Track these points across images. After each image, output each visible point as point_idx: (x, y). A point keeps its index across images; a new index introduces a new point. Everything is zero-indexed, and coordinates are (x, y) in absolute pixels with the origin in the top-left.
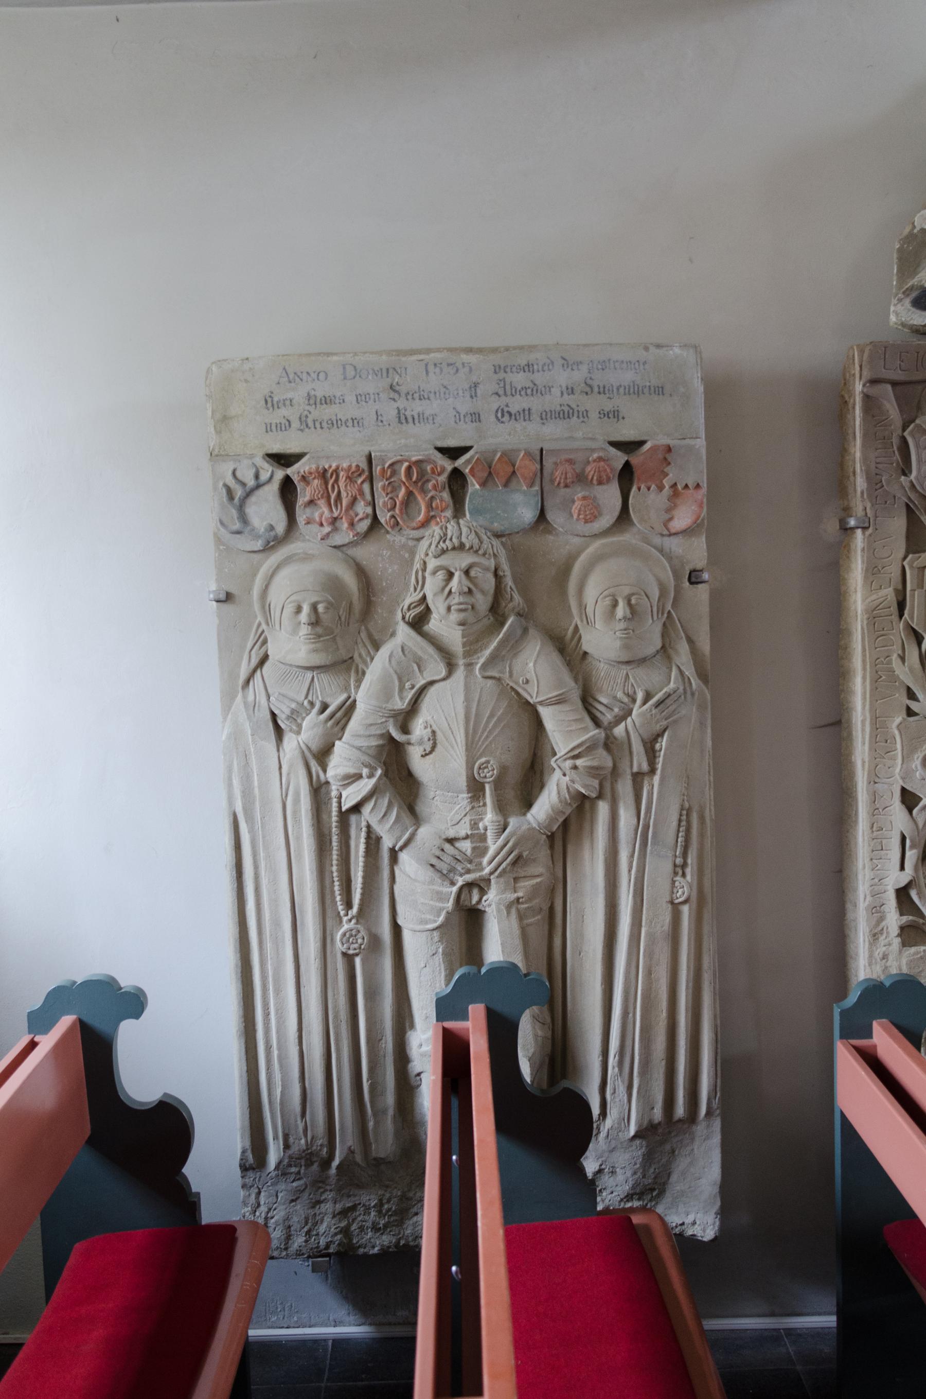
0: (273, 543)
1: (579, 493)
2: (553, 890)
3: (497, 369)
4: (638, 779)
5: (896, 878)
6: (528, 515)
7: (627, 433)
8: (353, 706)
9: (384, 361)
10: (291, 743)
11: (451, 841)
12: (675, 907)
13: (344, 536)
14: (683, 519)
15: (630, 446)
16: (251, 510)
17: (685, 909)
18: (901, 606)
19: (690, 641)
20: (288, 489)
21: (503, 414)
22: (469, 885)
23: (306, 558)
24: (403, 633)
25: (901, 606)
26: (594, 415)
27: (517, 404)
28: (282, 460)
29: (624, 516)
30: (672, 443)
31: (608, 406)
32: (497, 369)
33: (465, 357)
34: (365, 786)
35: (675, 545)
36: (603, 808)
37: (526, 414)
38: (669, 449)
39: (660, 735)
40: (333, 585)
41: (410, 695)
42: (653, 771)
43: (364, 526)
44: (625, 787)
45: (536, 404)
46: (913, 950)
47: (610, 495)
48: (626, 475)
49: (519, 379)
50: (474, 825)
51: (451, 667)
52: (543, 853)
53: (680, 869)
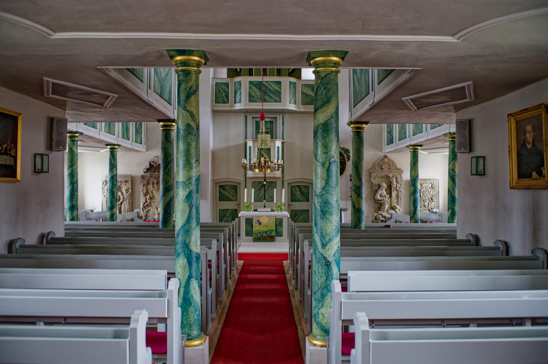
0: (105, 185)
4: (126, 200)
5: (142, 207)
6: (120, 184)
7: (126, 179)
10: (106, 197)
14: (129, 185)
15: (126, 180)
20: (106, 182)
25: (142, 190)
28: (106, 181)
29: (126, 185)
35: (129, 186)
36: (124, 202)
37: (120, 178)
44: (125, 200)
45: (120, 178)
47: (125, 183)
48: (126, 182)
53: (128, 206)
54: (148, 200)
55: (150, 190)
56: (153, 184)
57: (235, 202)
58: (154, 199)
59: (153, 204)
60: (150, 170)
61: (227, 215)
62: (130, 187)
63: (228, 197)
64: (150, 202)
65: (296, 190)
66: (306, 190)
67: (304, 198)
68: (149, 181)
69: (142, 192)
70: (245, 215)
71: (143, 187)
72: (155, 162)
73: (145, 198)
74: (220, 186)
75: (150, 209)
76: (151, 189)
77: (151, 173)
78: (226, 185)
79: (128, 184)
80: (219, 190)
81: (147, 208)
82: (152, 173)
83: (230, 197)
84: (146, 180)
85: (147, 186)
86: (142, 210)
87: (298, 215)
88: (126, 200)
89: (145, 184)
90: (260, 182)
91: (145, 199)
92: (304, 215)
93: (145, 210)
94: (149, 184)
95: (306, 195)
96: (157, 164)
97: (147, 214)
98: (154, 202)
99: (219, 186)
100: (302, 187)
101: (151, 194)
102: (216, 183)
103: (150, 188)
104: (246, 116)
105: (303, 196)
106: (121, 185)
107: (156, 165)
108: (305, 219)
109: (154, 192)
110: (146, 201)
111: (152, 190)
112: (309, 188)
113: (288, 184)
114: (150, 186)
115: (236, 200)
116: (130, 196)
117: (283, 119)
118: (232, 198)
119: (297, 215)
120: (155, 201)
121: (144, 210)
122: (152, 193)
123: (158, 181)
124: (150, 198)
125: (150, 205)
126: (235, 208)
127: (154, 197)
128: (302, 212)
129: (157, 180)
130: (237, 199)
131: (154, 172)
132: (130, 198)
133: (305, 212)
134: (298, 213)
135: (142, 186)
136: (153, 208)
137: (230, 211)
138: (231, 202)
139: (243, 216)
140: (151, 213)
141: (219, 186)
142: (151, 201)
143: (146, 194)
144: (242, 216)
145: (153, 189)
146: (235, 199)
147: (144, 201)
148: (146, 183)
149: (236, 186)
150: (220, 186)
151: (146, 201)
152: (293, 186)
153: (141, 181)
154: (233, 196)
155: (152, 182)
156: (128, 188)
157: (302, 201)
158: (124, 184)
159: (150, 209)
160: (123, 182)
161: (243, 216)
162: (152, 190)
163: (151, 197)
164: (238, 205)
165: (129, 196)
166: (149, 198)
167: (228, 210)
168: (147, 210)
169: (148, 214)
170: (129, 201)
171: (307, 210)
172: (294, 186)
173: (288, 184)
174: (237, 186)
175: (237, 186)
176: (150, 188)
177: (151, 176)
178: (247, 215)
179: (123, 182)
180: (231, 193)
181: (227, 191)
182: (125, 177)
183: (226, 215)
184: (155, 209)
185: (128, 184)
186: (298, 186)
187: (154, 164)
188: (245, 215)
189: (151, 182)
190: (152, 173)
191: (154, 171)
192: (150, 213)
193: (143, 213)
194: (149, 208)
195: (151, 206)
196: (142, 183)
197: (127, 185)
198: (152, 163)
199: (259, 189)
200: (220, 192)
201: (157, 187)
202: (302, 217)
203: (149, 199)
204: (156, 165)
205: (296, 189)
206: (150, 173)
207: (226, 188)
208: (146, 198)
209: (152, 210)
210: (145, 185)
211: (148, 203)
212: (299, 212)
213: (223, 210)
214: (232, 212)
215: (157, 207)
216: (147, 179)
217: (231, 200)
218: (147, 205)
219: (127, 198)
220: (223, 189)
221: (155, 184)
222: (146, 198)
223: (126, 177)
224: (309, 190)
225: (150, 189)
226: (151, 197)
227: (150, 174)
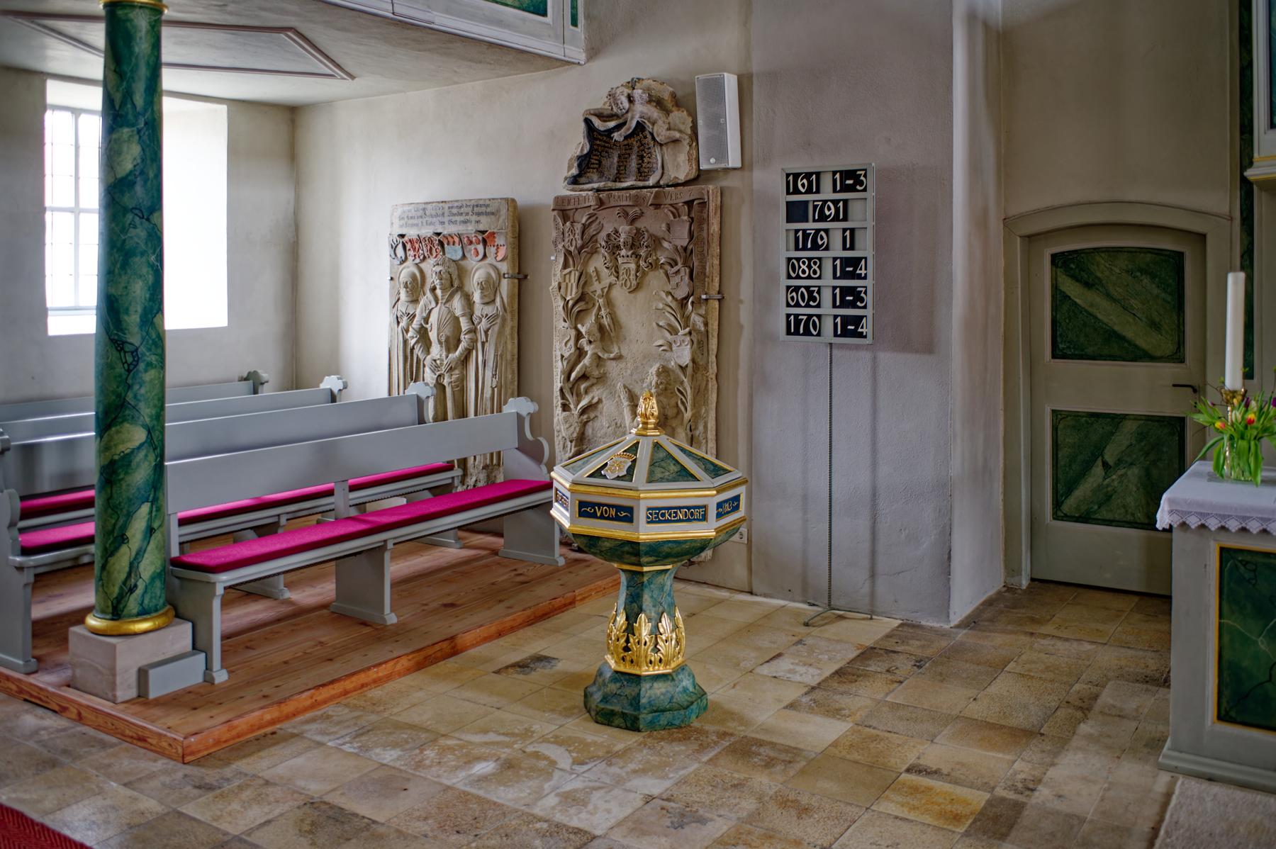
0: (403, 262)
1: (472, 247)
2: (462, 380)
3: (449, 208)
6: (460, 255)
7: (481, 228)
8: (415, 316)
9: (424, 206)
11: (435, 361)
12: (493, 389)
13: (417, 261)
16: (397, 251)
17: (496, 389)
18: (560, 288)
19: (502, 298)
21: (450, 222)
22: (440, 376)
23: (408, 267)
24: (429, 294)
25: (560, 288)
26: (473, 222)
27: (454, 219)
28: (402, 236)
29: (485, 256)
30: (495, 231)
31: (478, 219)
32: (449, 208)
33: (441, 204)
34: (415, 340)
35: (499, 265)
36: (474, 352)
38: (494, 233)
39: (489, 329)
40: (414, 277)
41: (427, 311)
42: (487, 341)
43: (422, 257)
45: (458, 218)
46: (565, 413)
47: (480, 248)
48: (485, 242)
49: (455, 211)
50: (441, 356)
51: (437, 303)
52: (460, 367)
53: (494, 375)
54: (587, 348)
55: (597, 287)
56: (614, 249)
57: (1167, 372)
58: (618, 337)
59: (613, 368)
60: (600, 162)
61: (1110, 455)
62: (504, 268)
63: (1112, 336)
64: (598, 360)
68: (592, 230)
69: (559, 298)
70: (1213, 524)
71: (565, 266)
72: (611, 117)
73: (573, 333)
74: (1059, 260)
75: (600, 401)
76: (605, 283)
77: (602, 184)
79: (493, 250)
80: (1055, 288)
81: (586, 392)
82: (610, 184)
83: (1129, 333)
84: (578, 227)
85: (586, 264)
86: (560, 402)
88: (483, 344)
89: (572, 249)
91: (572, 343)
93: (576, 407)
94: (594, 252)
96: (624, 124)
97: (585, 424)
98: (619, 358)
99: (1054, 257)
101: (603, 312)
102: (1030, 239)
103: (596, 270)
106: (464, 257)
107: (624, 132)
109: (619, 294)
110: (580, 353)
111: (611, 286)
114: (598, 263)
115: (1177, 357)
116: (504, 320)
118: (1144, 340)
120: (624, 353)
121: (572, 406)
122: (609, 303)
123: (638, 230)
124: (598, 335)
125: (596, 373)
126: (1168, 411)
127: (620, 327)
129: (633, 222)
130: (1180, 344)
131: (617, 179)
132: (501, 333)
135: (561, 260)
136: (613, 394)
137: (1130, 427)
138: (1139, 370)
139: (1193, 522)
140: (605, 424)
141: (1054, 257)
142: (600, 354)
143: (576, 309)
144: (1184, 525)
145: (613, 279)
146: (1168, 348)
147: (569, 351)
148: (580, 242)
149: (1177, 259)
150: (1059, 260)
151: (580, 353)
153: (554, 234)
154: (1154, 326)
155: (609, 235)
156: (493, 275)
158: (477, 254)
159: (600, 401)
160: (471, 243)
161: (1193, 522)
162: (611, 286)
163: (601, 328)
164: (1190, 390)
165: (499, 321)
166: (589, 333)
167: (1116, 420)
168: (583, 403)
169: (589, 431)
170: (496, 350)
174: (1180, 256)
175: (1180, 256)
176: (596, 270)
177: (601, 203)
178: (1233, 525)
179: (471, 243)
180: (1135, 303)
181: (1108, 296)
182: (479, 214)
183: (1098, 451)
184: (626, 403)
185: (493, 250)
187: (612, 124)
188: (1213, 524)
189: (602, 238)
190: (610, 184)
191: (619, 172)
192: (597, 424)
193: (566, 420)
194: (596, 394)
195: (602, 379)
196: (560, 247)
197: (490, 260)
198: (597, 123)
200: (1059, 297)
201: (633, 266)
203: (590, 342)
204: (624, 132)
206: (595, 185)
207: (1101, 268)
208: (579, 335)
209: (607, 407)
210: (570, 253)
211: (586, 361)
213: (1076, 415)
214: (1141, 436)
215: (637, 391)
216: (583, 221)
217: (1138, 355)
218: (584, 377)
219: (486, 332)
220: (1075, 278)
221: (623, 252)
222: (579, 335)
223: (487, 214)
225: (599, 280)
226: (601, 328)
227: (598, 190)
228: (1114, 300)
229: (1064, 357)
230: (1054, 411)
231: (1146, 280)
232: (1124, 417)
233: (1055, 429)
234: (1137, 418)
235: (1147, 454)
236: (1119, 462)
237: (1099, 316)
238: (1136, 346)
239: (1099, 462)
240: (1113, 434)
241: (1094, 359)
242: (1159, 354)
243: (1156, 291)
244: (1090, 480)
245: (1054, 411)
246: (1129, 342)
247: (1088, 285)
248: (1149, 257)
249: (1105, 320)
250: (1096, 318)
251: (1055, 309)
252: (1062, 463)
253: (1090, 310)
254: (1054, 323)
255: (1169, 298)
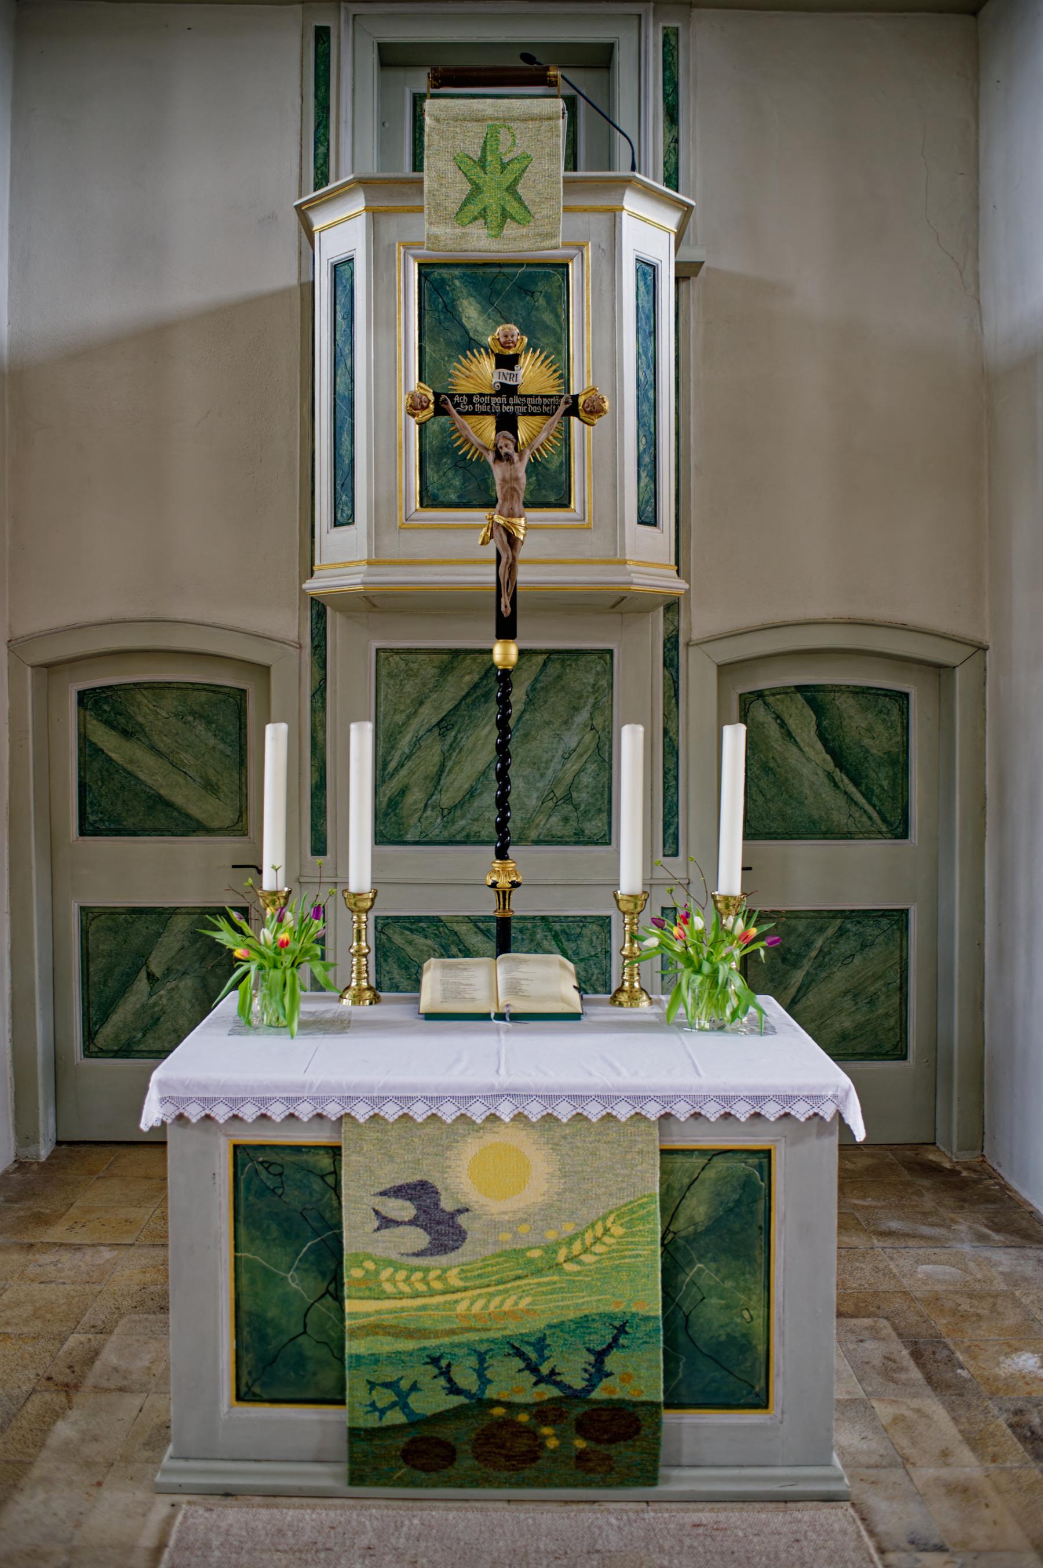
61: (156, 966)
63: (158, 802)
65: (789, 735)
66: (880, 728)
67: (862, 801)
78: (138, 686)
80: (84, 739)
83: (179, 800)
87: (807, 965)
90: (456, 653)
92: (858, 960)
95: (881, 778)
99: (82, 695)
100: (846, 704)
104: (322, 35)
105: (851, 789)
108: (872, 1001)
112: (905, 712)
113: (724, 670)
117: (670, 65)
118: (201, 807)
119: (795, 965)
128: (842, 932)
133: (871, 931)
134: (808, 945)
141: (82, 695)
146: (228, 816)
152: (760, 695)
154: (210, 787)
157: (848, 836)
167: (163, 915)
171: (885, 913)
172: (776, 692)
173: (724, 670)
180: (186, 757)
181: (153, 748)
183: (141, 959)
186: (811, 694)
199: (443, 726)
200: (88, 750)
202: (840, 978)
205: (792, 723)
212: (821, 930)
213: (112, 912)
220: (109, 724)
224: (906, 728)
228: (160, 754)
229: (96, 833)
230: (82, 909)
231: (200, 727)
232: (174, 911)
233: (84, 933)
234: (189, 911)
235: (203, 959)
236: (169, 971)
237: (142, 776)
238: (188, 816)
239: (143, 974)
240: (159, 935)
241: (134, 834)
242: (216, 824)
243: (212, 742)
244: (132, 999)
245: (82, 909)
246: (179, 810)
247: (126, 734)
248: (203, 696)
249: (149, 782)
250: (137, 778)
251: (82, 767)
252: (94, 978)
253: (129, 767)
254: (83, 788)
255: (228, 751)
